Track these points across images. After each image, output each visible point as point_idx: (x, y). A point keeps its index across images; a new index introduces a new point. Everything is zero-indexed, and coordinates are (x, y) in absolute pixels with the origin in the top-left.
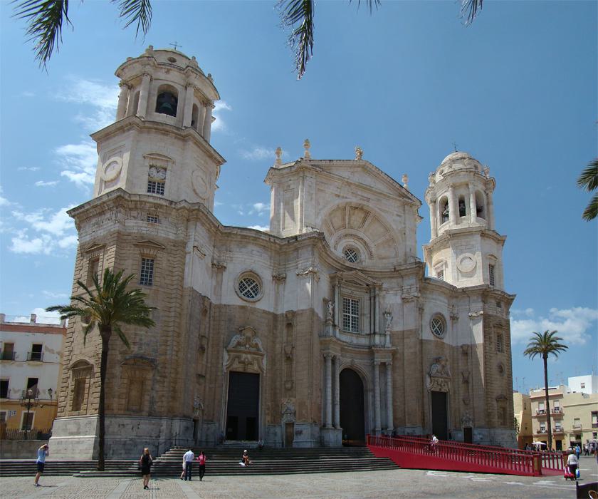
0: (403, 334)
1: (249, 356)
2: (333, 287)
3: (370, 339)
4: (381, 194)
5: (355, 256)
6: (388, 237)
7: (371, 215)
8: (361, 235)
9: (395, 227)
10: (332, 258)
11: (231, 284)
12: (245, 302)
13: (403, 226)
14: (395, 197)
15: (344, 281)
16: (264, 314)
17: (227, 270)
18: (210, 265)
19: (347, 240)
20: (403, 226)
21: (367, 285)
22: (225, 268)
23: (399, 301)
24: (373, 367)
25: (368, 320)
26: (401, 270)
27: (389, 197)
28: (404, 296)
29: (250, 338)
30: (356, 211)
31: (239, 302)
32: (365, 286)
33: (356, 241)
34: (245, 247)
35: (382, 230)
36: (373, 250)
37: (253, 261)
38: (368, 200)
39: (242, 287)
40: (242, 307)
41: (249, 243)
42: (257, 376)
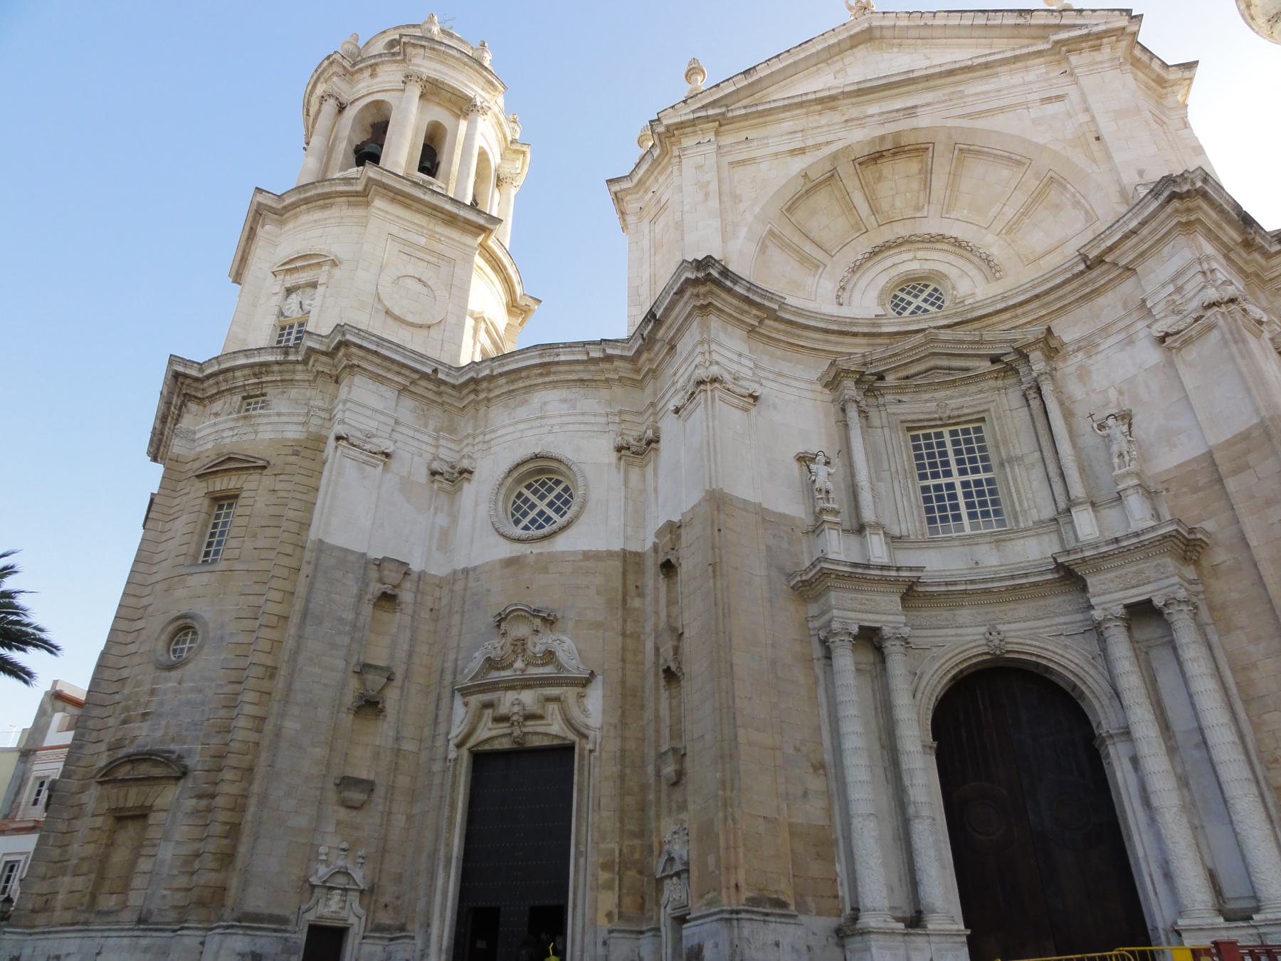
0: (1211, 457)
1: (528, 697)
2: (843, 410)
3: (1059, 532)
4: (951, 73)
5: (936, 299)
6: (1033, 184)
7: (940, 148)
8: (933, 226)
9: (1041, 137)
10: (816, 329)
11: (483, 509)
12: (518, 546)
13: (1084, 118)
14: (1008, 54)
15: (890, 379)
16: (587, 564)
17: (475, 477)
18: (422, 476)
19: (888, 263)
20: (1084, 118)
21: (995, 359)
22: (471, 473)
23: (1153, 356)
24: (1097, 630)
25: (1037, 473)
26: (1111, 249)
27: (987, 65)
28: (1159, 328)
29: (523, 641)
30: (886, 167)
31: (506, 550)
32: (986, 365)
33: (920, 254)
34: (526, 401)
35: (1005, 173)
36: (996, 250)
37: (546, 429)
38: (911, 111)
39: (519, 509)
40: (511, 562)
41: (529, 389)
42: (563, 753)
